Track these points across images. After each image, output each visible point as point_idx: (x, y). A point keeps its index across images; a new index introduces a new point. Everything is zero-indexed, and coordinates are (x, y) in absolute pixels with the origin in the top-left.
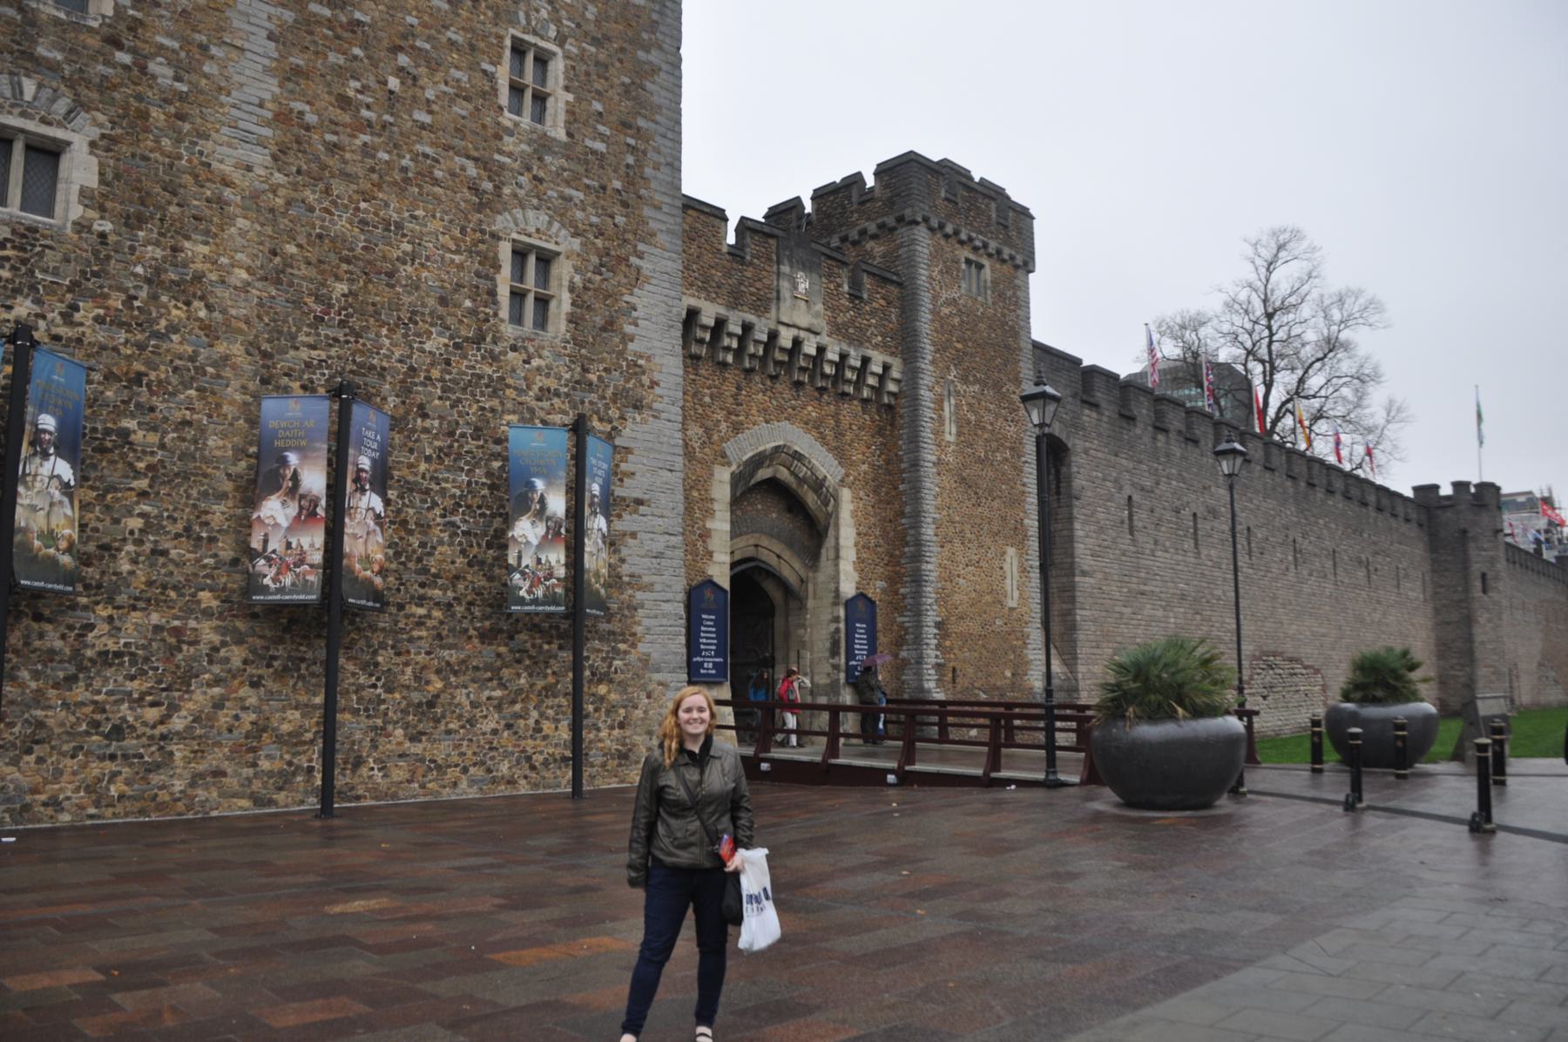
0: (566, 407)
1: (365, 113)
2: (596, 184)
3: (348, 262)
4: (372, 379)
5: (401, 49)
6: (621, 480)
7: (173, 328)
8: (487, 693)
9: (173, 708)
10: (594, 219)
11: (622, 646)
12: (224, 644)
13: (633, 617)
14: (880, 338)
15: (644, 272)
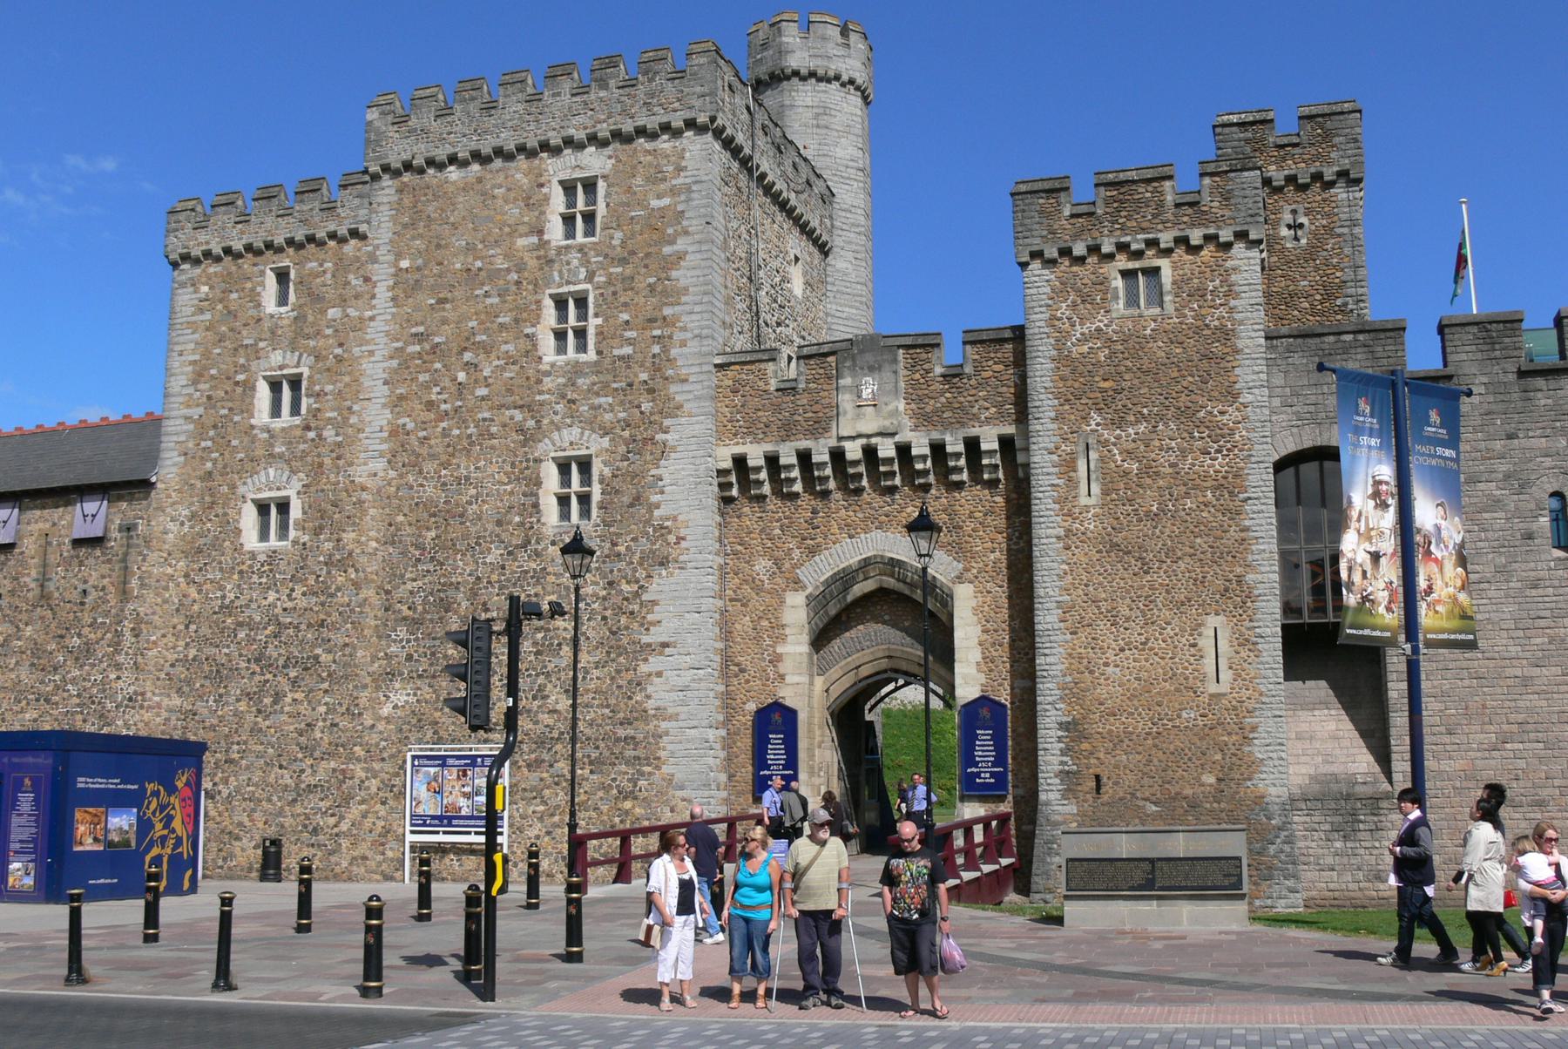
1: (443, 407)
2: (624, 384)
3: (434, 515)
5: (465, 349)
6: (647, 629)
7: (338, 589)
8: (532, 808)
9: (342, 818)
10: (622, 415)
11: (647, 769)
12: (367, 778)
13: (657, 743)
15: (671, 443)
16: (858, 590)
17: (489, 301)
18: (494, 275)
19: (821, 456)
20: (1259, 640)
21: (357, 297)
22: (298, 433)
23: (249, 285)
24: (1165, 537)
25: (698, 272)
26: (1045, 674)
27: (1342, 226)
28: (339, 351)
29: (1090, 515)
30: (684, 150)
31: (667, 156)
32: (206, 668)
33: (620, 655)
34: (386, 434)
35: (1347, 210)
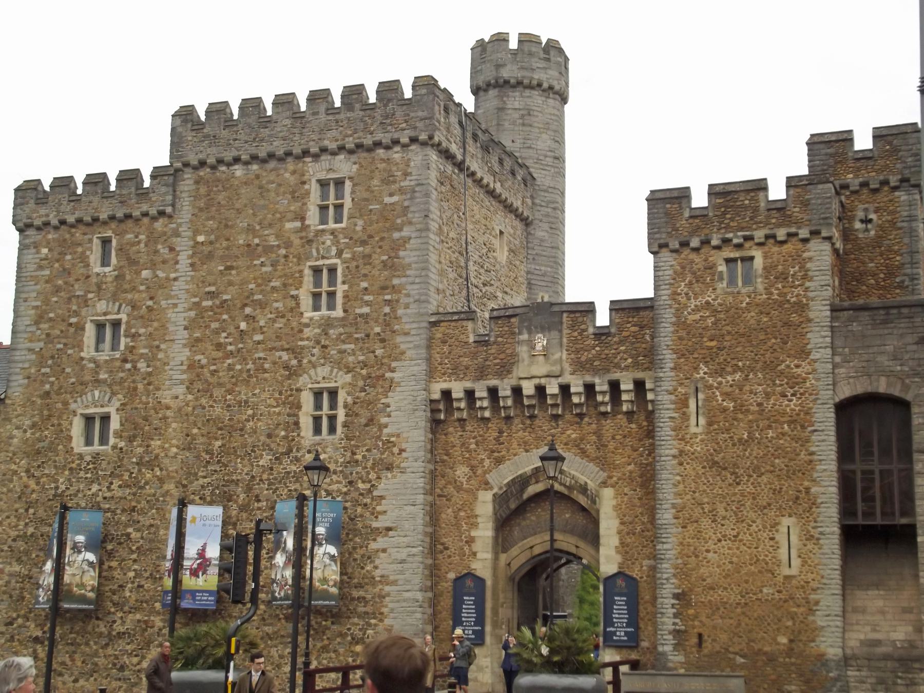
0: (341, 478)
1: (229, 348)
2: (363, 335)
3: (221, 429)
4: (232, 487)
5: (246, 305)
6: (376, 517)
7: (147, 483)
9: (143, 657)
10: (361, 358)
11: (373, 621)
13: (382, 602)
14: (630, 360)
15: (396, 380)
16: (533, 489)
17: (264, 269)
18: (268, 249)
19: (505, 391)
20: (822, 537)
21: (164, 262)
22: (118, 364)
23: (80, 249)
24: (751, 458)
25: (417, 253)
26: (662, 557)
27: (903, 221)
28: (150, 303)
29: (698, 440)
30: (409, 159)
31: (397, 164)
32: (42, 543)
33: (356, 536)
34: (185, 367)
35: (907, 208)
